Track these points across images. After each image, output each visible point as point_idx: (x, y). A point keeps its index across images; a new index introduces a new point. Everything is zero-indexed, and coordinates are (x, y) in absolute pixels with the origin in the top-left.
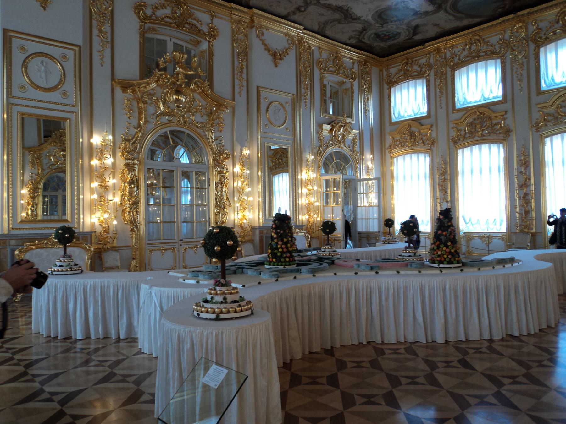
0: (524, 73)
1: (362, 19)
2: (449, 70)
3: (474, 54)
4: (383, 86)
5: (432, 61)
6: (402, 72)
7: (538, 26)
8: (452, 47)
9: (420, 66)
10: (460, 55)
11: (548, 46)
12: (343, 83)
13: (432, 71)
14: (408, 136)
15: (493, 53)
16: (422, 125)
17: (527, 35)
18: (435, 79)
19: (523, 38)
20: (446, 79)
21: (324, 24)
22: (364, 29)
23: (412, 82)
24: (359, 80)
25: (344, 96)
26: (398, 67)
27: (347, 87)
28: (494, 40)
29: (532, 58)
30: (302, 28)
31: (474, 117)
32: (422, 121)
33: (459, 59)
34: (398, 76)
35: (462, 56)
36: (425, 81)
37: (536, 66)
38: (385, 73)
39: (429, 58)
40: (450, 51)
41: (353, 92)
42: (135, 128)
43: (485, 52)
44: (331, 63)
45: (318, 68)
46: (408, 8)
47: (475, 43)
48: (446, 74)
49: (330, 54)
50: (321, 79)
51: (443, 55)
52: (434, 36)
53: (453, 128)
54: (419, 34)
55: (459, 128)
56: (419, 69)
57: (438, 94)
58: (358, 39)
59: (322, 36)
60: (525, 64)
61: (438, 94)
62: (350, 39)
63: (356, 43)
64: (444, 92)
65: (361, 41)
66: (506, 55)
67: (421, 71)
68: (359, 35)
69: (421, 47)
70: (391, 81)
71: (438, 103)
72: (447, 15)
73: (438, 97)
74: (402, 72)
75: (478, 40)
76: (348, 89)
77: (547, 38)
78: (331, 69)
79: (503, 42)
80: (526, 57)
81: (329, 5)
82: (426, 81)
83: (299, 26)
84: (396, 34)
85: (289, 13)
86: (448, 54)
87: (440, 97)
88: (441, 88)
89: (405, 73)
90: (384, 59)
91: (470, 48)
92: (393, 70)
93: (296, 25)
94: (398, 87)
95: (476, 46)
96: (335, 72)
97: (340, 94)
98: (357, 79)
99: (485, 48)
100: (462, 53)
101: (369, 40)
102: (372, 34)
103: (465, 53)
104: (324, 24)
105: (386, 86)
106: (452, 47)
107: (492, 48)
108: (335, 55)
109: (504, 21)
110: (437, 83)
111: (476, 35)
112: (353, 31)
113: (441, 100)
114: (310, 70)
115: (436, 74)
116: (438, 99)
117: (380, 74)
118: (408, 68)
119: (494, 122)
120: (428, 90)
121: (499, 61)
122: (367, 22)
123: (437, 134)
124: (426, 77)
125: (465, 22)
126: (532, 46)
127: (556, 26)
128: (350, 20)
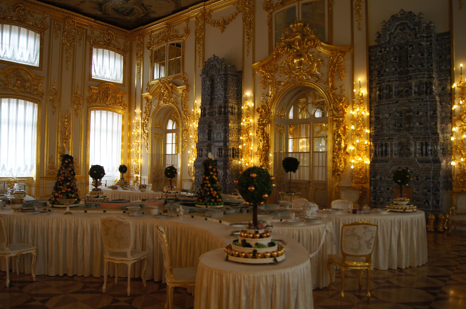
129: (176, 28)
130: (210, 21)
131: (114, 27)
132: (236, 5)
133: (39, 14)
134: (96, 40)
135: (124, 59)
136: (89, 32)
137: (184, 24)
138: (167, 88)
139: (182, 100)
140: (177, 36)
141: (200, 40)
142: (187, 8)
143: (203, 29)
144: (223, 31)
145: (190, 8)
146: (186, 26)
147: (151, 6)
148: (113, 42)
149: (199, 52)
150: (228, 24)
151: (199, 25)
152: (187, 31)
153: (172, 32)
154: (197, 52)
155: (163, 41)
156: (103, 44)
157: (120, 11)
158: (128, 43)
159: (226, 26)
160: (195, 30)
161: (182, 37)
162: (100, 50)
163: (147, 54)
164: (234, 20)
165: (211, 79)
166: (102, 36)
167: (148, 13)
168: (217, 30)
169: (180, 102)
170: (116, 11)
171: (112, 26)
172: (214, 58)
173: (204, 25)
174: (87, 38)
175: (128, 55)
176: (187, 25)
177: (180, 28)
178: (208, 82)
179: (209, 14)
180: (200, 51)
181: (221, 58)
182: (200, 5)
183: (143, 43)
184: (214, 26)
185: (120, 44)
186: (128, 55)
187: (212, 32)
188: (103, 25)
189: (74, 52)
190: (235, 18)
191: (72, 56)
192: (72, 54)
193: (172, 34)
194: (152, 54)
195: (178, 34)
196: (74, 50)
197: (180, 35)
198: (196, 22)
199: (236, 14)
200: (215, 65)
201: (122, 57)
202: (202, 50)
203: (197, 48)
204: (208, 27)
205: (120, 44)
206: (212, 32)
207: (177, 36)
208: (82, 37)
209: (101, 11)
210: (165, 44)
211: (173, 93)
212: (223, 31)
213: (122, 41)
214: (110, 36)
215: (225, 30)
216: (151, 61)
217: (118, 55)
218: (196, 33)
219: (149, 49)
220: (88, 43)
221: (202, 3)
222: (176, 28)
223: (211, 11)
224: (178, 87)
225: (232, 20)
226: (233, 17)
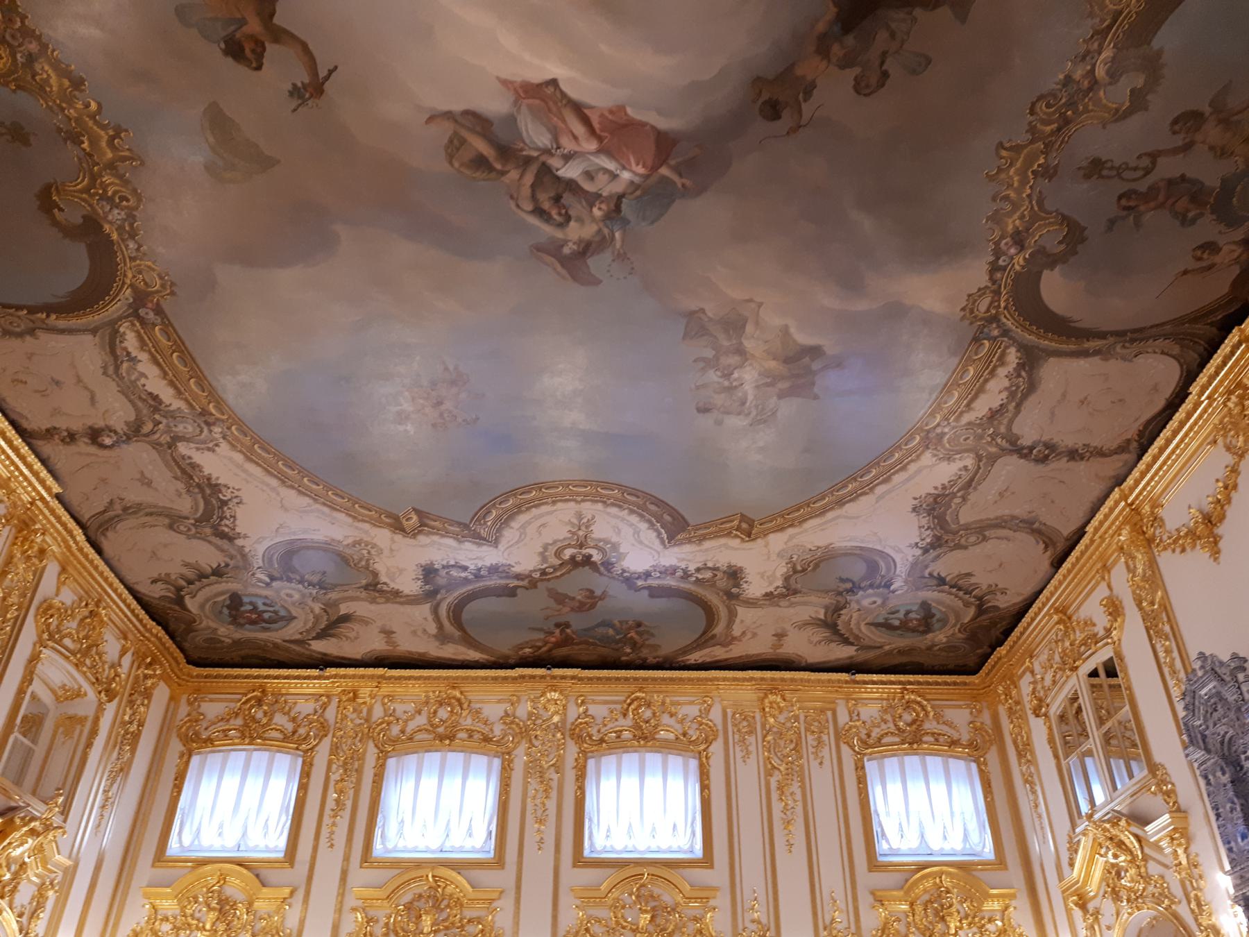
0: (551, 805)
1: (239, 542)
2: (372, 753)
3: (441, 730)
4: (167, 744)
5: (331, 714)
6: (239, 722)
7: (587, 710)
8: (391, 698)
9: (294, 720)
10: (406, 721)
11: (604, 760)
12: (78, 694)
13: (327, 742)
14: (210, 908)
15: (487, 739)
16: (264, 885)
17: (564, 721)
18: (330, 763)
19: (556, 725)
20: (359, 771)
21: (125, 509)
22: (218, 572)
23: (260, 757)
24: (121, 701)
25: (60, 738)
26: (232, 705)
27: (81, 712)
28: (493, 711)
29: (570, 775)
30: (56, 489)
31: (418, 891)
32: (267, 874)
33: (403, 732)
34: (222, 726)
35: (412, 726)
36: (300, 761)
37: (576, 797)
38: (184, 710)
39: (324, 707)
40: (384, 704)
41: (94, 732)
42: (106, 411)
43: (471, 733)
44: (74, 624)
45: (36, 621)
46: (367, 567)
47: (449, 705)
48: (362, 758)
49: (81, 600)
50: (34, 659)
51: (365, 710)
52: (358, 657)
53: (354, 910)
54: (333, 640)
55: (372, 913)
56: (290, 727)
57: (330, 804)
58: (179, 589)
59: (89, 540)
60: (554, 784)
61: (330, 804)
62: (154, 581)
63: (162, 598)
64: (349, 804)
65: (180, 601)
66: (515, 752)
67: (294, 732)
68: (190, 582)
69: (315, 672)
70: (197, 734)
71: (325, 832)
72: (430, 618)
73: (328, 812)
74: (239, 722)
75: (459, 700)
76: (82, 720)
77: (602, 741)
78: (67, 641)
79: (512, 722)
80: (558, 768)
81: (194, 466)
82: (304, 762)
83: (50, 481)
84: (282, 618)
85: (50, 433)
86: (378, 712)
87: (335, 816)
88: (340, 792)
89: (246, 725)
90: (196, 671)
91: (435, 712)
92: (212, 709)
93: (44, 473)
94: (214, 759)
95: (452, 712)
96: (73, 653)
97: (48, 725)
98: (117, 700)
99: (468, 722)
100: (412, 718)
101: (202, 606)
102: (222, 593)
103: (421, 720)
104: (125, 509)
105: (176, 746)
106: (391, 698)
107: (486, 730)
108: (91, 607)
109: (523, 677)
110: (335, 777)
111: (454, 688)
112: (187, 565)
113: (334, 824)
114: (17, 618)
115: (335, 750)
116: (327, 820)
117: (168, 705)
118: (260, 715)
119: (468, 914)
120: (303, 788)
121: (497, 762)
122: (244, 556)
123: (302, 922)
124: (306, 751)
125: (449, 651)
126: (572, 750)
127: (622, 722)
128: (208, 530)
129: (1083, 613)
130: (1165, 537)
131: (920, 678)
132: (1220, 441)
133: (692, 703)
134: (869, 736)
135: (982, 773)
136: (843, 717)
137: (1102, 592)
138: (1121, 845)
139: (1182, 882)
140: (1095, 639)
141: (1160, 622)
142: (1080, 533)
143: (1154, 578)
144: (1215, 553)
145: (1090, 529)
146: (1107, 593)
147: (969, 575)
148: (930, 725)
149: (1172, 666)
150: (1222, 518)
151: (1140, 571)
152: (1114, 609)
153: (1078, 633)
154: (1166, 670)
155: (1064, 670)
156: (897, 739)
157: (897, 623)
158: (986, 718)
159: (1220, 530)
160: (1134, 593)
161: (1108, 631)
162: (891, 763)
163: (1038, 730)
164: (1233, 494)
165: (1223, 757)
166: (888, 717)
167: (980, 599)
168: (1200, 555)
169: (1177, 891)
170: (886, 626)
171: (911, 678)
172: (1202, 667)
173: (1152, 564)
174: (841, 736)
175: (992, 756)
176: (1109, 586)
177: (1092, 610)
178: (1219, 774)
179: (1156, 520)
180: (1173, 659)
181: (1225, 657)
182: (1109, 503)
183: (1017, 703)
184: (1183, 550)
185: (954, 728)
186: (992, 756)
187: (1183, 573)
188: (883, 683)
189: (803, 788)
190: (1235, 487)
191: (800, 804)
192: (799, 796)
193: (1079, 636)
194: (1050, 728)
195: (1096, 629)
196: (802, 781)
197: (1102, 633)
198: (1126, 563)
199: (1234, 470)
200: (1218, 694)
201: (974, 766)
202: (1176, 654)
203: (1162, 655)
204: (1168, 562)
205: (954, 728)
206: (1183, 573)
207: (1095, 639)
208: (825, 737)
209: (846, 642)
210: (1073, 680)
211: (1146, 858)
212: (1215, 553)
213: (959, 717)
214: (914, 710)
215: (1221, 544)
216: (1056, 757)
217: (958, 766)
218: (1139, 605)
219: (1037, 716)
220: (845, 749)
221: (1116, 494)
222: (1083, 613)
223: (1156, 504)
224: (1147, 828)
225: (1229, 500)
226: (1226, 487)
